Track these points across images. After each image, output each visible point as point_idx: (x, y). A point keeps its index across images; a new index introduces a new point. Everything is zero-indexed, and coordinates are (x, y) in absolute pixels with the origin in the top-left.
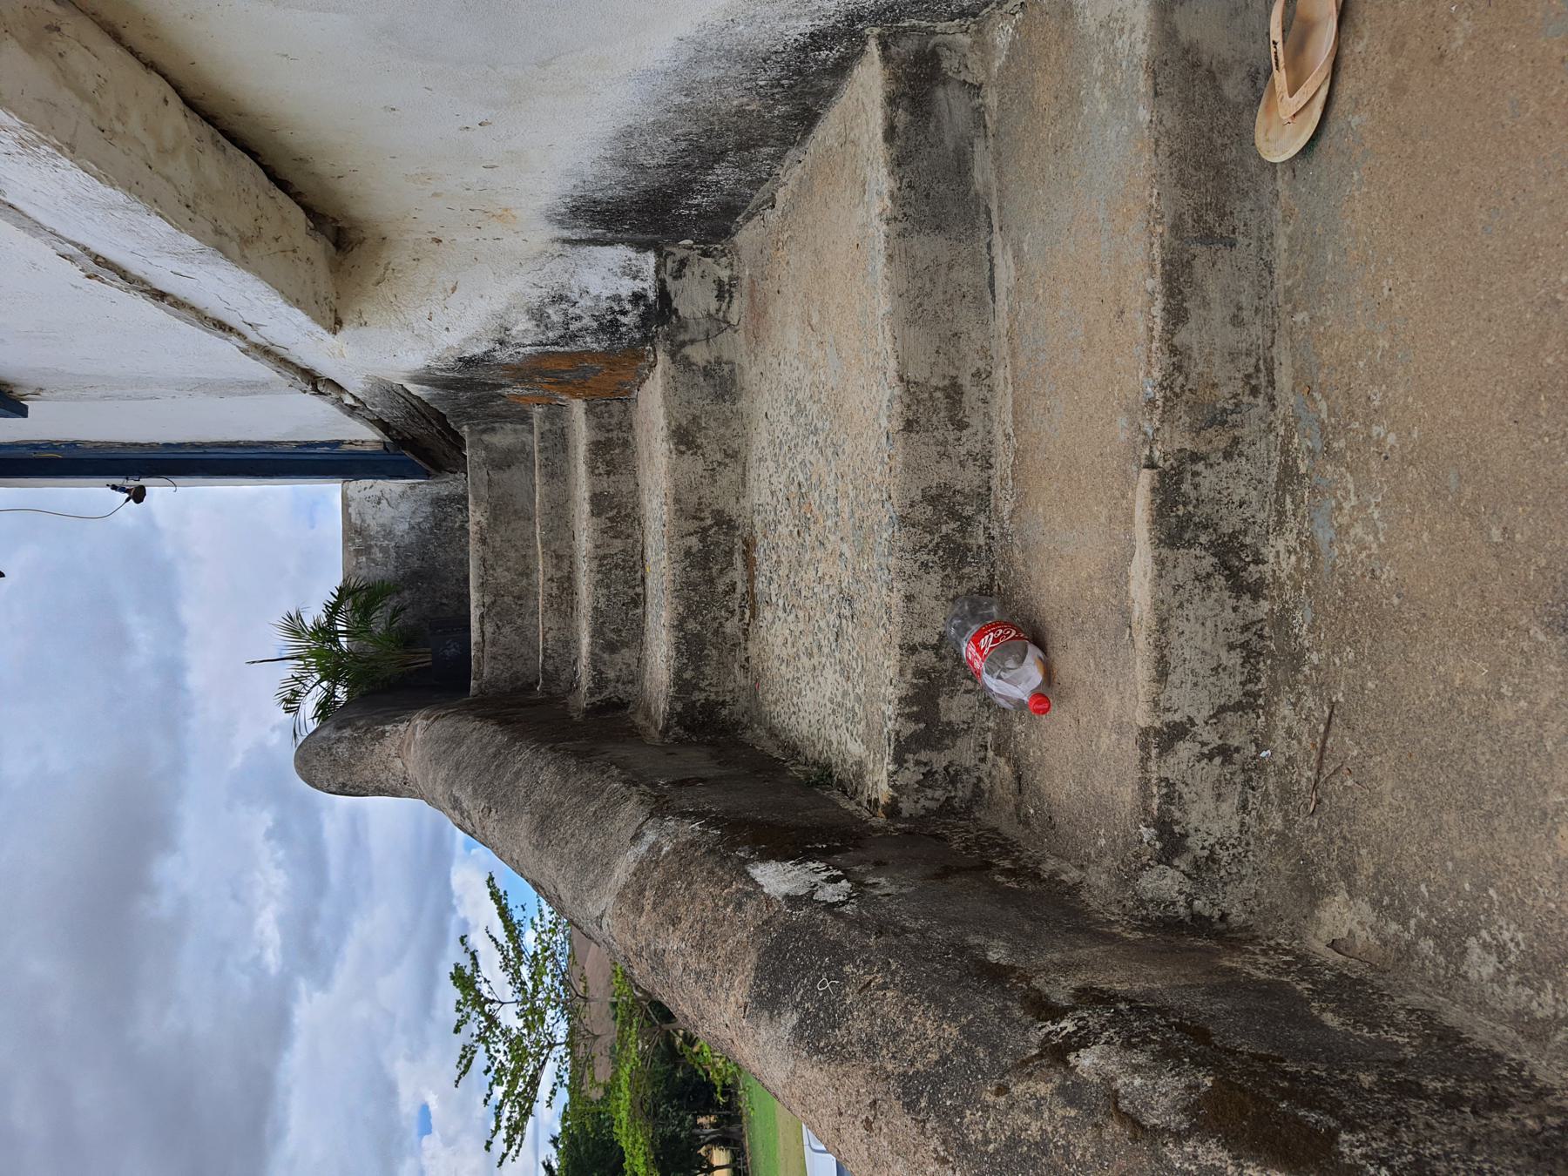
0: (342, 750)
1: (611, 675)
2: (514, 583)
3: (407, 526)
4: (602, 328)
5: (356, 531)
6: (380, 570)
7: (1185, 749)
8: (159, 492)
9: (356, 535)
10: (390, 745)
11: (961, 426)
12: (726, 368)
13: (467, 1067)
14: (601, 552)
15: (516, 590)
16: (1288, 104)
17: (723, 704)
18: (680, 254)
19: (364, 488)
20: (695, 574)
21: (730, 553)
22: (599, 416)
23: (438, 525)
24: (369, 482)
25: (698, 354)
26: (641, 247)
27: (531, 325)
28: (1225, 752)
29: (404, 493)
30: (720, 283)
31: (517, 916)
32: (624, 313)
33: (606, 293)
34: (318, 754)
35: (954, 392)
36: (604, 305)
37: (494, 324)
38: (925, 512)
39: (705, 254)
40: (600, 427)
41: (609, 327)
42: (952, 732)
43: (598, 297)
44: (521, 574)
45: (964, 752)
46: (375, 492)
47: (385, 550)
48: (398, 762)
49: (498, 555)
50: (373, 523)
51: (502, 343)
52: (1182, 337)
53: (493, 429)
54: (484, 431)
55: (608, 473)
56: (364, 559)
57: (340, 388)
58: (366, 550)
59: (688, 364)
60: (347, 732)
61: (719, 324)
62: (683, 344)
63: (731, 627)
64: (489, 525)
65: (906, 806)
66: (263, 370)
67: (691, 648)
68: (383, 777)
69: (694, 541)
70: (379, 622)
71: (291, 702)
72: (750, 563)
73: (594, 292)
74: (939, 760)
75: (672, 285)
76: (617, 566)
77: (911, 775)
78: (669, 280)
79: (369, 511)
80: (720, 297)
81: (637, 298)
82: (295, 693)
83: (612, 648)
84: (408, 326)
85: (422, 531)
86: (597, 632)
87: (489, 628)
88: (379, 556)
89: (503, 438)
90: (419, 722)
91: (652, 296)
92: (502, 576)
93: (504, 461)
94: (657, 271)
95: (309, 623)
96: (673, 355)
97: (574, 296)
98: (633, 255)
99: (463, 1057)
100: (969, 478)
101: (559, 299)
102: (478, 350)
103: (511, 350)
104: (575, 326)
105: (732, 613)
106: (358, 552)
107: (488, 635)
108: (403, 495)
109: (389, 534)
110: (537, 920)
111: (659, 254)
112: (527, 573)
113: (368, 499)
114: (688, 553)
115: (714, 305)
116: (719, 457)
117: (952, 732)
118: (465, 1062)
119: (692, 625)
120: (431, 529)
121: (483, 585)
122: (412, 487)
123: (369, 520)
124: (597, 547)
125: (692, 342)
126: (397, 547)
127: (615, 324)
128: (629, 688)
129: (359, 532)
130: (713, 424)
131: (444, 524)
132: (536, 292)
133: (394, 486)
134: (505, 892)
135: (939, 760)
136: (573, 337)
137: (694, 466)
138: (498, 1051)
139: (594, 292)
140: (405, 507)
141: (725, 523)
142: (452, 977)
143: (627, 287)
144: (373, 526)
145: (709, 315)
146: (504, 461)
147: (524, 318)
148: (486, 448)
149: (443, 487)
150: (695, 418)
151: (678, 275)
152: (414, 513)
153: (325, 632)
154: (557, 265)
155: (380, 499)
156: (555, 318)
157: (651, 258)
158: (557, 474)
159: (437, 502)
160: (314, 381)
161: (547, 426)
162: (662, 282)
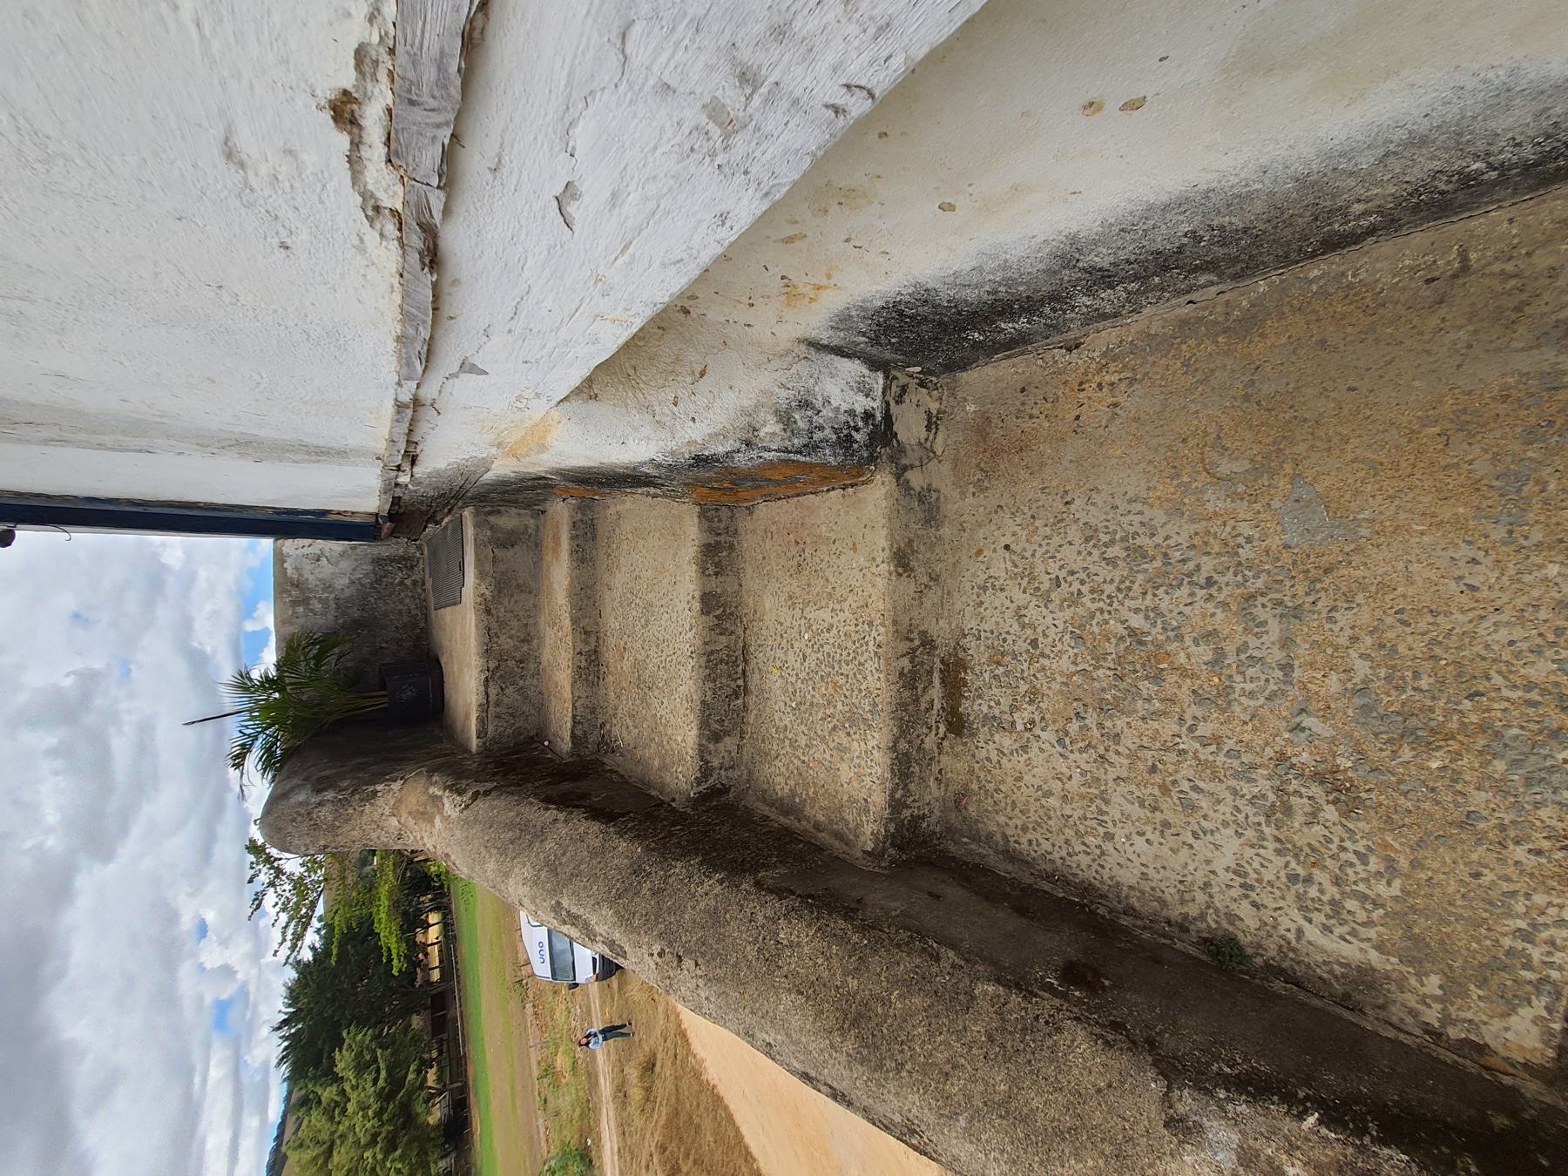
0: (325, 813)
1: (716, 763)
2: (517, 649)
3: (347, 581)
4: (839, 441)
5: (292, 584)
6: (321, 619)
9: (290, 589)
10: (383, 805)
12: (934, 495)
13: (258, 906)
14: (708, 648)
15: (518, 655)
17: (923, 817)
18: (903, 380)
20: (906, 694)
21: (930, 672)
22: (710, 520)
23: (378, 581)
24: (307, 542)
27: (778, 428)
29: (344, 552)
30: (929, 414)
32: (857, 429)
33: (844, 407)
34: (294, 820)
36: (843, 418)
37: (744, 421)
39: (922, 384)
40: (711, 530)
43: (837, 409)
44: (523, 641)
48: (394, 821)
49: (502, 624)
50: (311, 578)
51: (748, 444)
53: (499, 512)
54: (490, 513)
55: (717, 574)
56: (302, 609)
60: (329, 795)
62: (905, 469)
64: (493, 597)
68: (374, 835)
73: (835, 404)
75: (894, 409)
76: (722, 661)
78: (892, 403)
79: (307, 567)
80: (928, 428)
81: (868, 416)
84: (649, 409)
85: (362, 585)
88: (318, 606)
91: (879, 416)
92: (506, 643)
94: (884, 393)
97: (818, 404)
98: (866, 372)
99: (255, 900)
101: (805, 404)
103: (754, 454)
104: (818, 436)
105: (930, 728)
106: (295, 603)
107: (492, 698)
108: (343, 554)
113: (306, 556)
114: (901, 674)
115: (924, 434)
116: (925, 580)
118: (256, 902)
119: (903, 746)
120: (372, 584)
122: (353, 548)
123: (307, 574)
124: (706, 644)
125: (912, 467)
126: (336, 599)
127: (849, 438)
128: (730, 773)
129: (297, 585)
130: (922, 548)
131: (385, 580)
132: (784, 393)
137: (908, 587)
138: (284, 891)
139: (835, 404)
140: (345, 565)
142: (247, 848)
143: (861, 403)
144: (312, 580)
145: (920, 443)
147: (772, 419)
148: (492, 528)
150: (911, 541)
152: (354, 570)
154: (802, 368)
155: (319, 556)
156: (802, 424)
159: (377, 561)
161: (579, 516)
162: (888, 404)
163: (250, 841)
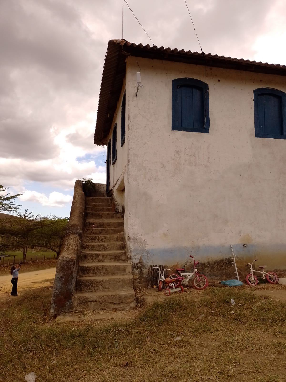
0: (80, 184)
7: (92, 230)
8: (106, 165)
9: (100, 185)
11: (108, 226)
16: (120, 233)
19: (105, 186)
20: (98, 214)
25: (114, 215)
26: (122, 212)
28: (91, 233)
31: (12, 200)
35: (109, 225)
38: (103, 224)
41: (116, 209)
42: (90, 225)
45: (88, 226)
46: (105, 187)
47: (99, 188)
48: (78, 189)
52: (110, 230)
57: (114, 188)
58: (99, 186)
59: (114, 214)
60: (81, 185)
61: (117, 217)
63: (94, 217)
65: (85, 223)
66: (114, 184)
67: (92, 214)
69: (100, 214)
70: (91, 187)
71: (84, 179)
72: (99, 218)
74: (88, 225)
77: (87, 223)
80: (119, 217)
81: (118, 211)
82: (84, 179)
83: (91, 209)
86: (92, 208)
87: (91, 199)
89: (110, 201)
90: (83, 192)
91: (119, 212)
93: (108, 201)
95: (91, 181)
96: (114, 213)
100: (105, 226)
102: (115, 200)
108: (104, 190)
109: (100, 188)
110: (12, 203)
111: (121, 213)
112: (97, 203)
113: (104, 187)
117: (90, 225)
121: (95, 198)
126: (99, 189)
133: (106, 189)
134: (17, 197)
135: (88, 225)
136: (116, 206)
140: (103, 190)
141: (102, 217)
143: (119, 210)
144: (101, 187)
146: (108, 201)
149: (105, 195)
151: (120, 214)
153: (90, 182)
154: (121, 205)
157: (121, 212)
158: (106, 206)
159: (104, 194)
160: (114, 187)
163: (2, 187)
